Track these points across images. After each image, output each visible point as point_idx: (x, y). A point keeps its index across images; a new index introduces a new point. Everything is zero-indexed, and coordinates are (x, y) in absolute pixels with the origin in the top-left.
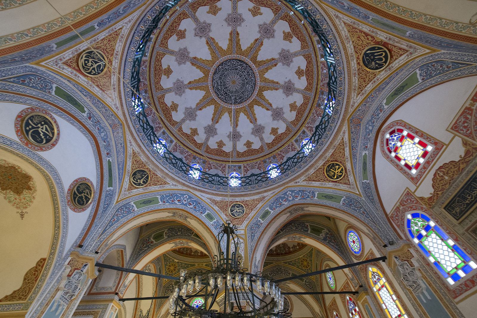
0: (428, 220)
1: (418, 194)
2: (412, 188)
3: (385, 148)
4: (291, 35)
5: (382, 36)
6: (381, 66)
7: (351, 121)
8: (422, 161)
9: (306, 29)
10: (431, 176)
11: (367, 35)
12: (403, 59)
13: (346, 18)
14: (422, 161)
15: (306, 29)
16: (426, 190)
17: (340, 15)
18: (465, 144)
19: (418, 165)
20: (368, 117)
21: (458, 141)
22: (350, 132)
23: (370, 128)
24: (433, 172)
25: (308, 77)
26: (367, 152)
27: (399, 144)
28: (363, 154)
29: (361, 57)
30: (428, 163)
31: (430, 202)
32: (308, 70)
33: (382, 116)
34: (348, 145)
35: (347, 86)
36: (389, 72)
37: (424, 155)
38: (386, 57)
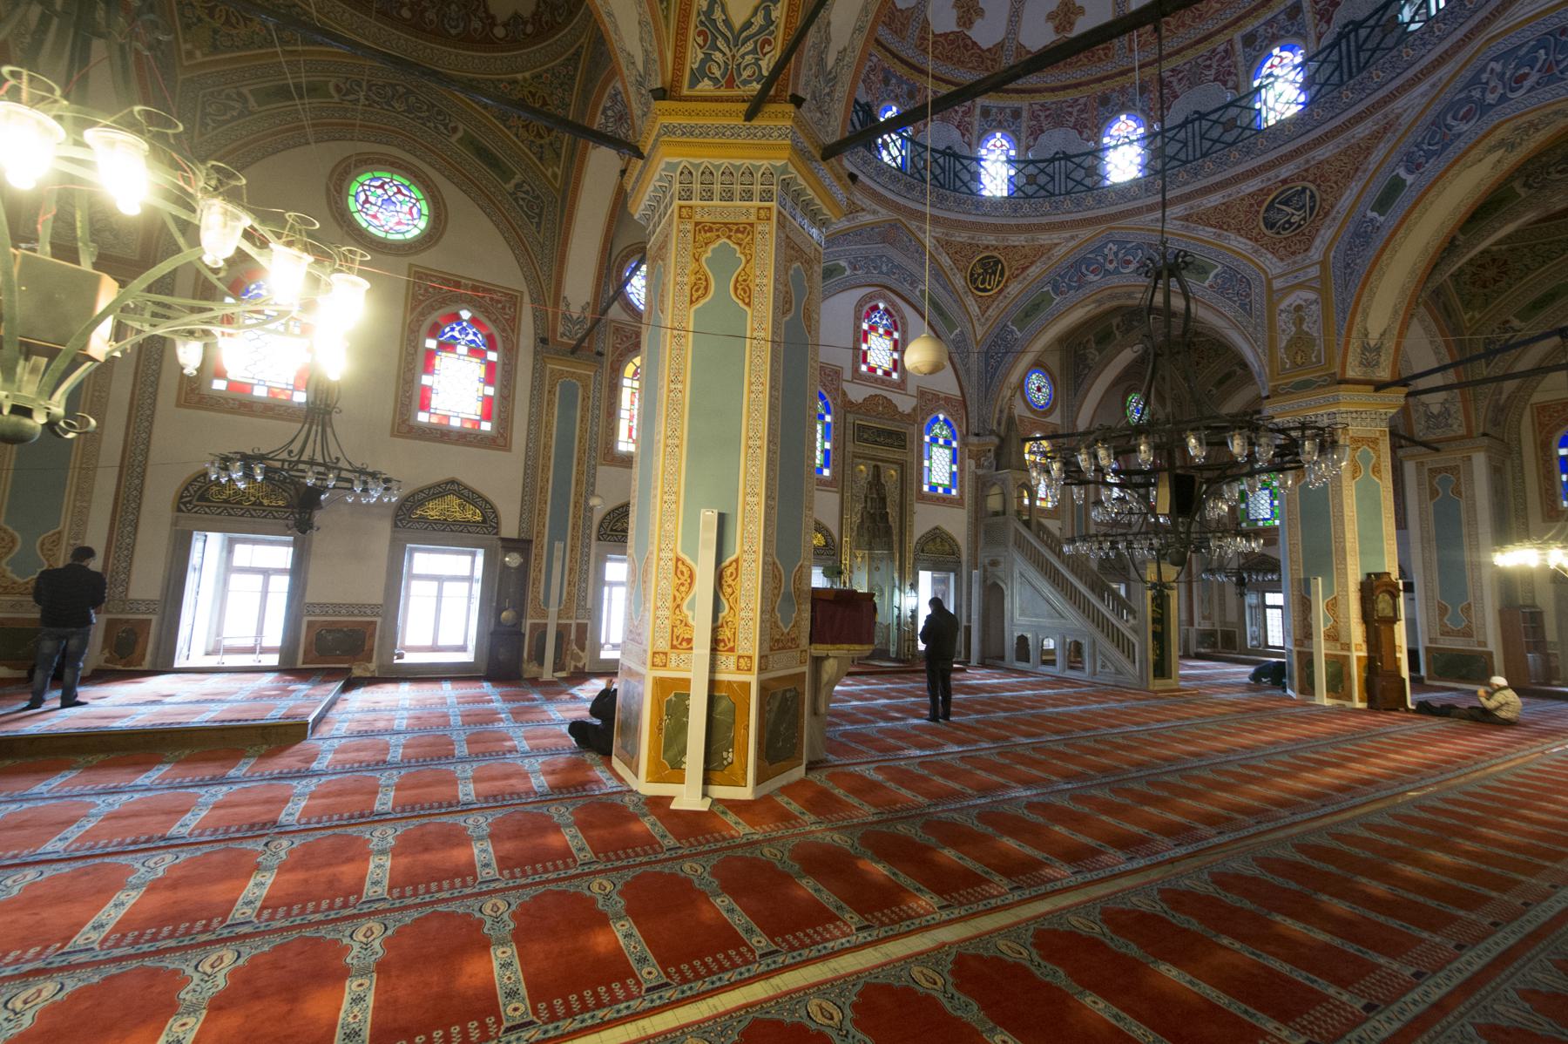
0: (828, 412)
1: (846, 386)
2: (847, 375)
3: (866, 308)
4: (1064, 29)
5: (1014, 288)
6: (974, 281)
7: (893, 225)
8: (880, 372)
9: (1053, 90)
10: (872, 391)
11: (1024, 269)
12: (974, 309)
13: (1064, 250)
14: (880, 372)
15: (1053, 90)
16: (857, 393)
17: (1072, 244)
18: (914, 409)
19: (873, 370)
20: (898, 257)
21: (913, 402)
22: (873, 226)
23: (884, 269)
24: (878, 392)
25: (952, 42)
26: (848, 272)
27: (881, 331)
28: (843, 263)
29: (995, 254)
30: (883, 382)
31: (848, 406)
32: (965, 46)
33: (905, 288)
34: (853, 224)
35: (953, 216)
36: (961, 291)
37: (887, 373)
38: (985, 290)
